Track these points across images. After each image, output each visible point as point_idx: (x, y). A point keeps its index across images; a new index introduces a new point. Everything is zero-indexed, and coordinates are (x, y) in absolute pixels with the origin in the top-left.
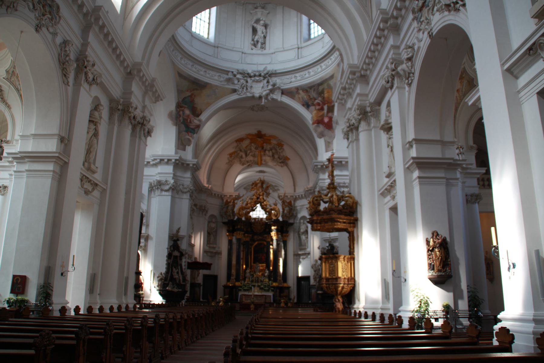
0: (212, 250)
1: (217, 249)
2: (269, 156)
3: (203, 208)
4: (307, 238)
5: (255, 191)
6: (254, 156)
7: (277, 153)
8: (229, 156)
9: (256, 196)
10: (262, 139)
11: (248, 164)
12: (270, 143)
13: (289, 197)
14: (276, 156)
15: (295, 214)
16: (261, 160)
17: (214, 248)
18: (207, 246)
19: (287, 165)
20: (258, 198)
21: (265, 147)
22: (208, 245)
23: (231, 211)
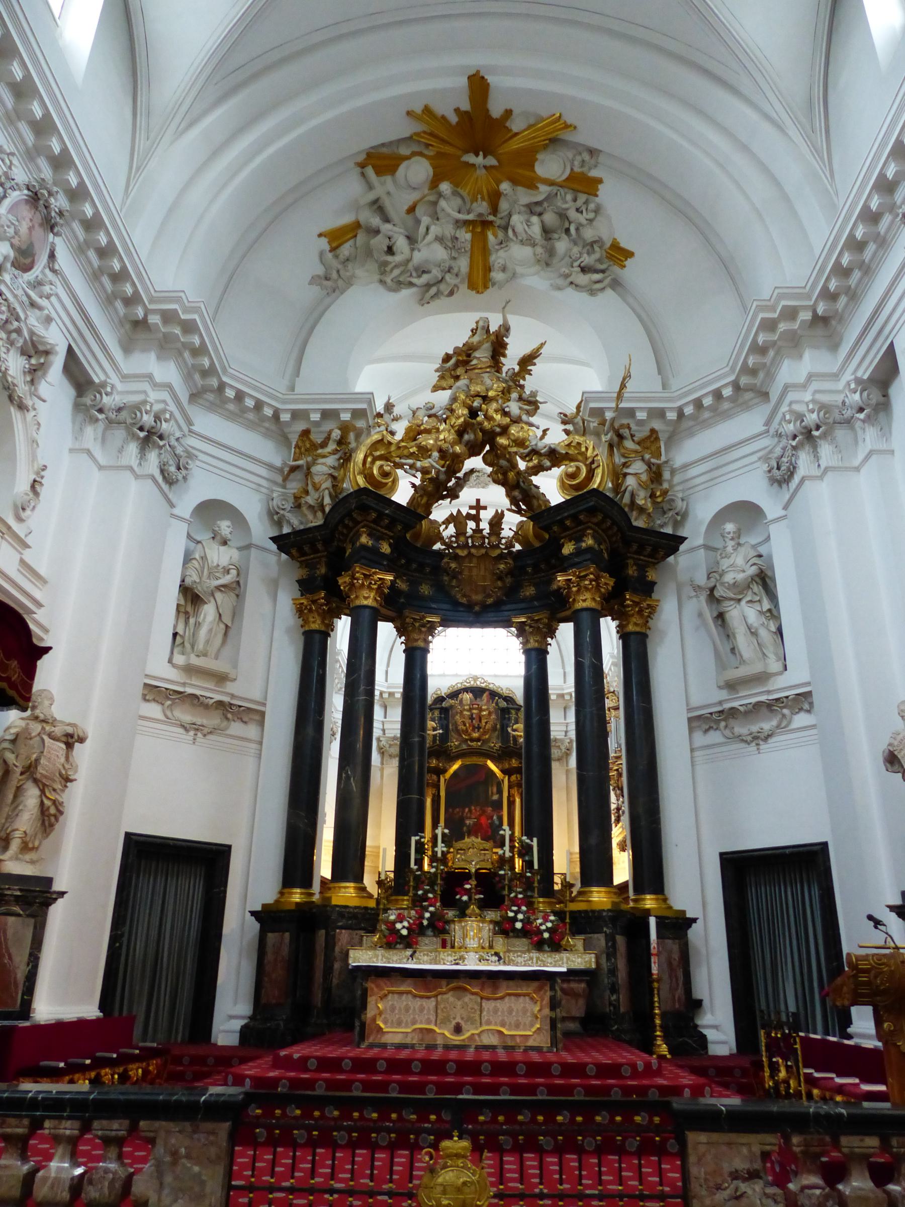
0: (197, 687)
1: (230, 687)
2: (530, 242)
3: (147, 420)
4: (773, 614)
5: (462, 382)
6: (450, 243)
7: (567, 231)
8: (324, 243)
9: (464, 404)
10: (491, 161)
11: (425, 278)
12: (531, 184)
13: (641, 415)
14: (562, 245)
15: (680, 505)
16: (488, 269)
17: (221, 678)
18: (170, 661)
19: (616, 284)
20: (473, 413)
21: (504, 205)
22: (179, 659)
23: (328, 484)
